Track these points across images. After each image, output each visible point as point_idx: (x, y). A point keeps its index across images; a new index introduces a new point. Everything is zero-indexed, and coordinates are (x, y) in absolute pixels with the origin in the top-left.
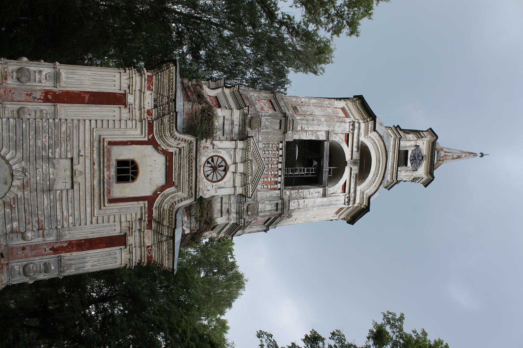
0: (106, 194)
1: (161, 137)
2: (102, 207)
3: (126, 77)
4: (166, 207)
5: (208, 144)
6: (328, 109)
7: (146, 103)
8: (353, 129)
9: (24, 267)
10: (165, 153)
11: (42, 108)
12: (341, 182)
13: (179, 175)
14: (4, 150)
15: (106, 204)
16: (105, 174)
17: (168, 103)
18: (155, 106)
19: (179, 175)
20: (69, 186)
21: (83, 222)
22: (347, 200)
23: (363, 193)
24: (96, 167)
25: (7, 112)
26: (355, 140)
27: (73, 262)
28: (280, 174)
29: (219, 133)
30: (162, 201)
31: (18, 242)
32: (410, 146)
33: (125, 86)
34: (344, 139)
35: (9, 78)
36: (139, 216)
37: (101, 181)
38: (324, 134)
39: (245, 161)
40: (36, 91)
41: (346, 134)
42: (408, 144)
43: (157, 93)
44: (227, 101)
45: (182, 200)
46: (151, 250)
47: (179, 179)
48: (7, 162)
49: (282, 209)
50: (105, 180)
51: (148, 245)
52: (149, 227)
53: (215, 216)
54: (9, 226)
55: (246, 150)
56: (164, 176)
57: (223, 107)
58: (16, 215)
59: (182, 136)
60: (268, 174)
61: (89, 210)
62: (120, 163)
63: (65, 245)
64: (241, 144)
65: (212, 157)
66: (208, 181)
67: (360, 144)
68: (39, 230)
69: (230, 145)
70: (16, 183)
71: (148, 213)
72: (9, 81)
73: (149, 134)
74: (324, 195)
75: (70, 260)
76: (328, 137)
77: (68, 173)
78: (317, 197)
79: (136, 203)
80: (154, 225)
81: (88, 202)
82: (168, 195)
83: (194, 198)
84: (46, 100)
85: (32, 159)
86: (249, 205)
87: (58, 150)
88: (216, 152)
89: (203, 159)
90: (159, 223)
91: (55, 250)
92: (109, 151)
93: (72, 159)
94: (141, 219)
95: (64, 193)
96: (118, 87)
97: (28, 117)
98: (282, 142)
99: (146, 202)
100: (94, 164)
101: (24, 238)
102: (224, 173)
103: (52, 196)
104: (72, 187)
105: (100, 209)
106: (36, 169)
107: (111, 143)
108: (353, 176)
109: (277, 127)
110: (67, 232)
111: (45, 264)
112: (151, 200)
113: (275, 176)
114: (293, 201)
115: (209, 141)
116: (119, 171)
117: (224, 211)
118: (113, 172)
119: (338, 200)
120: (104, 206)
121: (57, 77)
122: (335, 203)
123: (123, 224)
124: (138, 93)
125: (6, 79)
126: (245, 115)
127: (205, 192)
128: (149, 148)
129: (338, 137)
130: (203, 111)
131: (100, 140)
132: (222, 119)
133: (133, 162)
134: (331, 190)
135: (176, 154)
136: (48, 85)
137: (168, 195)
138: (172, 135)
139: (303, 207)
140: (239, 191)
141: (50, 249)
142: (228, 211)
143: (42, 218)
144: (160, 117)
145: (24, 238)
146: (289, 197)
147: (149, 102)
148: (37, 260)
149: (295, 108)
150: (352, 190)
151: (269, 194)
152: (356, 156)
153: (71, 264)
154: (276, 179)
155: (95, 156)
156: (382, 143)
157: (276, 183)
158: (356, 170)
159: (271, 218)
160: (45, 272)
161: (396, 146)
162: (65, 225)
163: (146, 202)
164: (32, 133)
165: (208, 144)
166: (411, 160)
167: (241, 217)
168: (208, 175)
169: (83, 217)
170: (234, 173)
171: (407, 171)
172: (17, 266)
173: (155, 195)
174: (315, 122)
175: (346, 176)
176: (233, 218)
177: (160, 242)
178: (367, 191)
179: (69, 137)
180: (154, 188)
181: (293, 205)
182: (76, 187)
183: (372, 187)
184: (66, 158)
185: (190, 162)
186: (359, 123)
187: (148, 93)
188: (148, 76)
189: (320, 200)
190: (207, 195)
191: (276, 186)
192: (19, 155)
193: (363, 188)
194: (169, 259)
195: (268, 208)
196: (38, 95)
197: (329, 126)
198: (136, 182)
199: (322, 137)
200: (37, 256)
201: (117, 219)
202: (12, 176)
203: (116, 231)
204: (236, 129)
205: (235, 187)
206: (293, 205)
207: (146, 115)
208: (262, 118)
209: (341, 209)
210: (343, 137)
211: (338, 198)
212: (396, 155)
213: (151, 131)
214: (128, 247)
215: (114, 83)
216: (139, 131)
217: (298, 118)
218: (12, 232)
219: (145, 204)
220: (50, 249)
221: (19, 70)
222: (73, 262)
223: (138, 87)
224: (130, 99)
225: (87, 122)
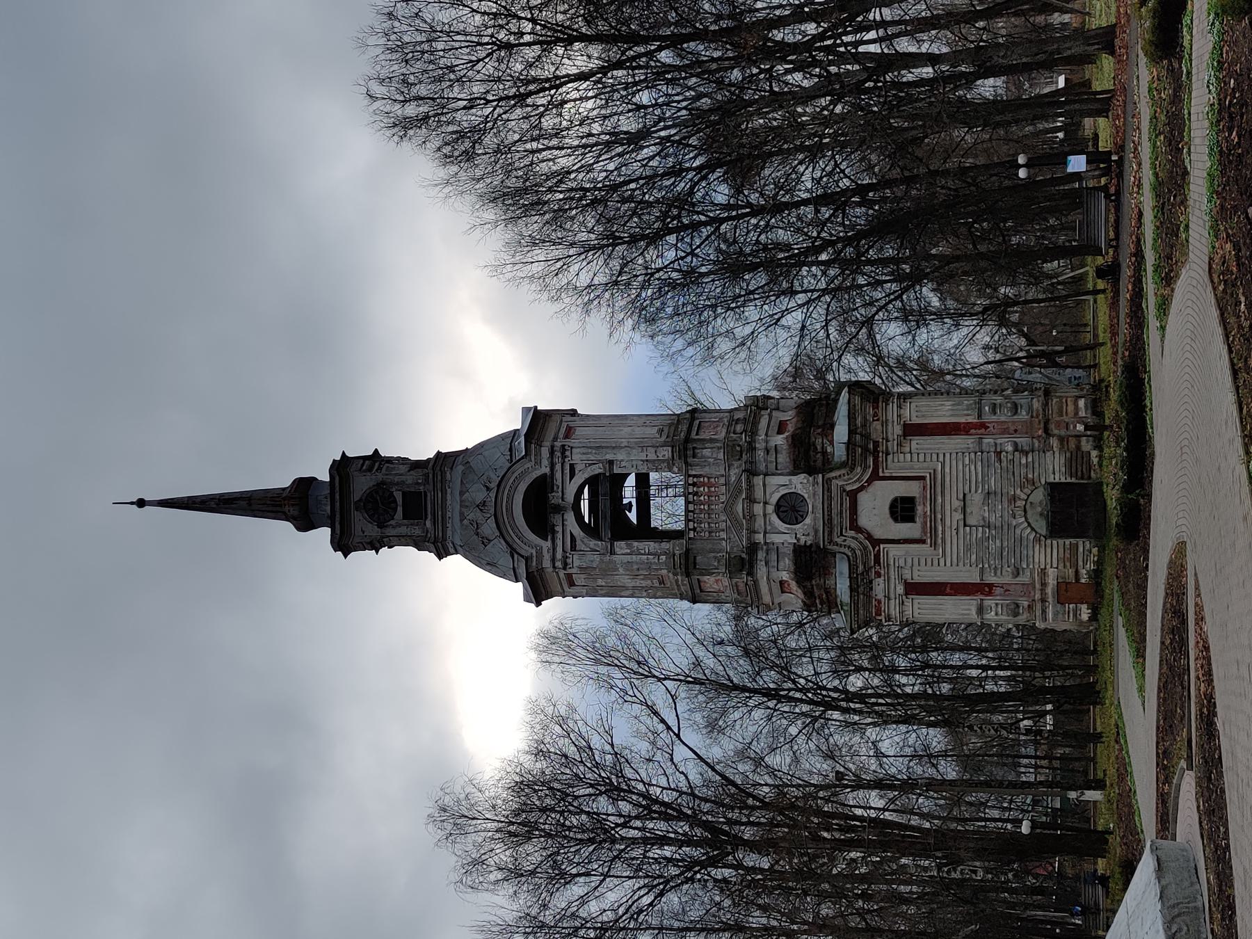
0: (929, 487)
1: (865, 548)
2: (932, 471)
3: (906, 613)
4: (859, 469)
5: (803, 539)
6: (603, 584)
7: (882, 586)
8: (565, 558)
9: (1016, 413)
10: (859, 530)
11: (995, 578)
13: (841, 505)
14: (1032, 537)
15: (928, 475)
16: (929, 509)
17: (858, 587)
18: (871, 582)
19: (841, 505)
20: (968, 497)
21: (954, 456)
22: (568, 453)
23: (538, 463)
24: (939, 516)
25: (1029, 574)
26: (559, 543)
27: (965, 412)
28: (691, 496)
29: (789, 550)
30: (862, 475)
31: (1023, 441)
32: (399, 525)
33: (908, 603)
34: (578, 542)
35: (1026, 606)
36: (890, 457)
37: (933, 501)
38: (617, 550)
39: (751, 517)
40: (1001, 595)
41: (575, 550)
42: (403, 530)
43: (870, 597)
44: (770, 589)
45: (840, 476)
46: (874, 416)
47: (842, 499)
48: (1029, 525)
49: (686, 449)
50: (928, 502)
51: (879, 422)
52: (876, 444)
53: (785, 447)
54: (1030, 459)
55: (752, 531)
56: (859, 503)
57: (777, 581)
58: (1023, 471)
59: (842, 550)
60: (709, 497)
61: (947, 470)
62: (911, 519)
63: (973, 431)
64: (759, 538)
65: (797, 523)
66: (802, 494)
67: (549, 537)
68: (1001, 452)
69: (776, 539)
70: (1020, 503)
71: (878, 461)
72: (1026, 604)
73: (879, 550)
74: (611, 463)
75: (968, 415)
76: (612, 545)
77: (968, 510)
78: (622, 461)
79: (894, 475)
80: (871, 446)
81: (947, 479)
82: (855, 482)
83: (825, 479)
84: (991, 586)
85: (1005, 527)
86: (739, 459)
87: (980, 535)
88: (791, 529)
89: (808, 520)
90: (865, 449)
91: (983, 426)
92: (925, 533)
93: (965, 525)
94: (887, 454)
95: (973, 489)
96: (916, 602)
97: (1009, 569)
98: (690, 539)
99: (881, 474)
100: (941, 520)
101: (1016, 444)
102: (780, 503)
103: (987, 487)
104: (964, 495)
105: (934, 470)
106: (1002, 517)
107: (923, 542)
108: (558, 488)
109: (699, 558)
110: (971, 446)
111: (995, 414)
112: (875, 477)
113: (696, 494)
114: (666, 457)
115: (802, 543)
116: (913, 509)
117: (773, 452)
118: (919, 509)
119: (584, 454)
120: (930, 474)
121: (981, 610)
122: (590, 451)
123: (908, 449)
124: (892, 596)
125: (1029, 606)
126: (750, 573)
127: (805, 481)
128: (878, 534)
129: (592, 546)
130: (810, 578)
131: (934, 545)
132: (780, 568)
133: (896, 520)
134: (597, 470)
135: (846, 529)
136: (989, 602)
137: (855, 482)
138: (853, 550)
139: (649, 448)
140: (758, 480)
141: (989, 427)
142: (767, 451)
143: (996, 464)
144: (867, 570)
145: (1016, 444)
146: (674, 464)
147: (879, 588)
148: (1003, 419)
149: (662, 582)
150: (558, 467)
151: (706, 470)
152: (557, 519)
153: (968, 410)
154: (695, 489)
155: (940, 528)
156: (509, 539)
157: (694, 484)
158: (555, 498)
159: (697, 434)
160: (995, 404)
161: (440, 528)
162: (973, 455)
163: (881, 474)
164: (1005, 554)
165: (803, 539)
166: (395, 501)
167: (749, 443)
168: (802, 501)
169: (954, 463)
170: (766, 503)
171: (397, 484)
172: (1023, 415)
173: (870, 481)
174: (635, 567)
176: (759, 443)
177: (864, 426)
178: (529, 465)
179: (968, 549)
180: (870, 489)
181: (666, 453)
182: (961, 496)
183: (519, 471)
184: (970, 526)
185: (830, 519)
186: (554, 567)
187: (881, 596)
188: (880, 615)
189: (620, 456)
190: (802, 477)
191: (695, 480)
192: (1018, 531)
193: (535, 469)
194: (854, 405)
195: (707, 452)
196: (998, 591)
197: (610, 561)
198: (892, 497)
199: (621, 546)
200: (1002, 422)
201: (915, 456)
202: (1025, 511)
203: (916, 443)
204: (761, 555)
205: (764, 485)
206: (666, 453)
207: (882, 572)
208: (724, 570)
209: (567, 436)
210: (579, 545)
211: (584, 457)
212: (440, 513)
213: (877, 557)
214: (902, 423)
215: (920, 606)
216: (891, 555)
217: (664, 572)
218: (1027, 453)
219: (883, 472)
220: (989, 427)
221: (1016, 614)
222: (965, 412)
223: (892, 602)
224: (900, 589)
225: (948, 564)
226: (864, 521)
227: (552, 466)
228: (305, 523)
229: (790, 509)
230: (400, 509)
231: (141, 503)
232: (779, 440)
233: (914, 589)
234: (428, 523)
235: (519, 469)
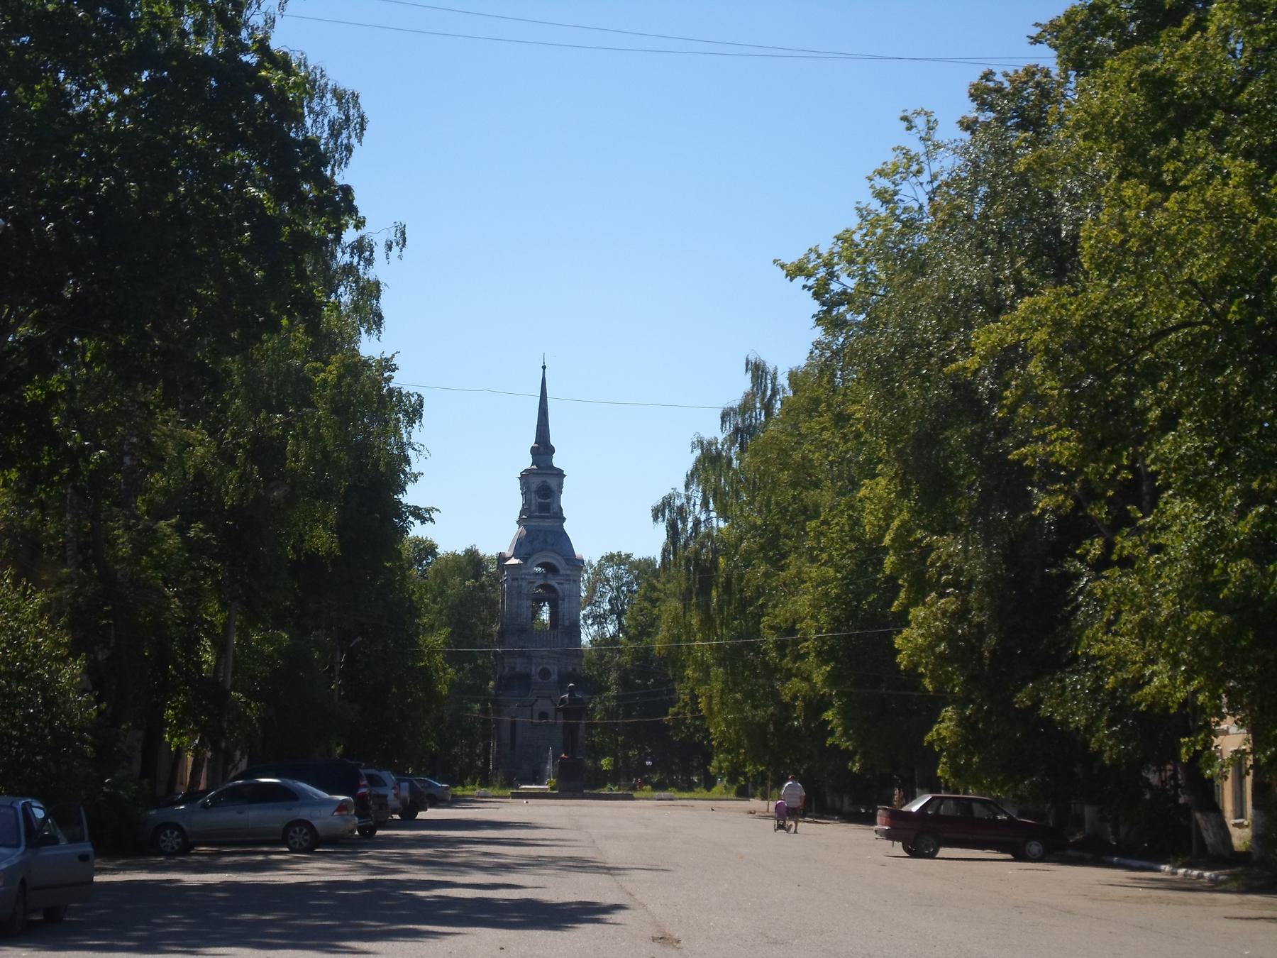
8: (526, 579)
12: (556, 586)
42: (533, 502)
74: (564, 600)
89: (540, 680)
189: (566, 605)
227: (563, 575)
229: (545, 673)
230: (543, 501)
231: (544, 368)
232: (570, 668)
234: (537, 514)
235: (563, 562)
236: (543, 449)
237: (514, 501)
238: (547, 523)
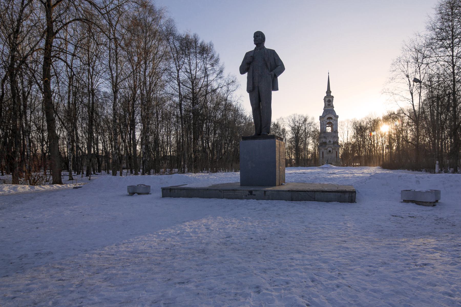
175: (331, 121)
226: (329, 148)
228: (327, 92)
229: (330, 141)
232: (336, 140)
233: (323, 152)
236: (329, 92)
237: (322, 105)
238: (330, 108)
